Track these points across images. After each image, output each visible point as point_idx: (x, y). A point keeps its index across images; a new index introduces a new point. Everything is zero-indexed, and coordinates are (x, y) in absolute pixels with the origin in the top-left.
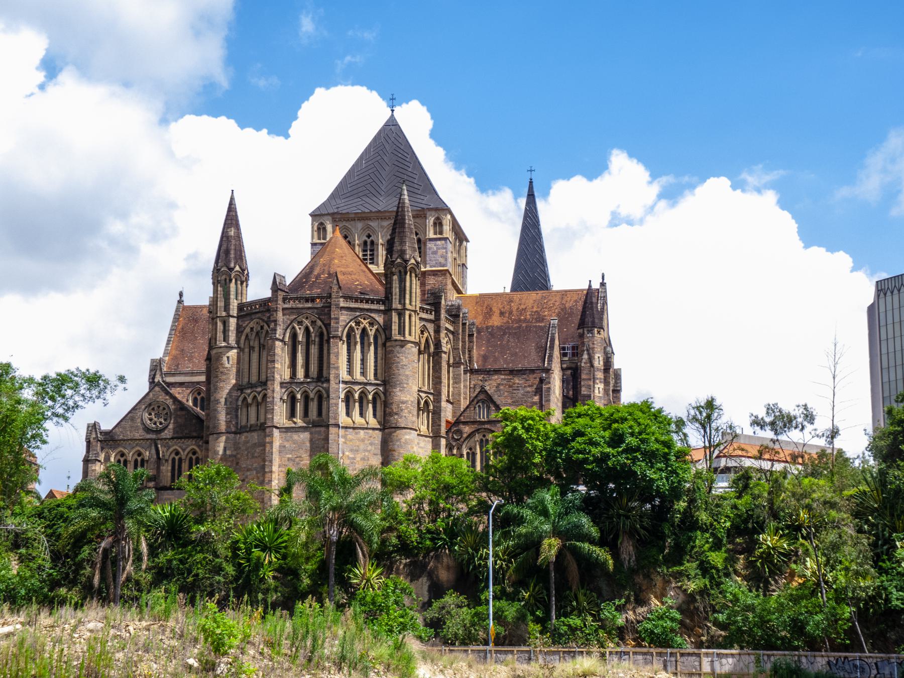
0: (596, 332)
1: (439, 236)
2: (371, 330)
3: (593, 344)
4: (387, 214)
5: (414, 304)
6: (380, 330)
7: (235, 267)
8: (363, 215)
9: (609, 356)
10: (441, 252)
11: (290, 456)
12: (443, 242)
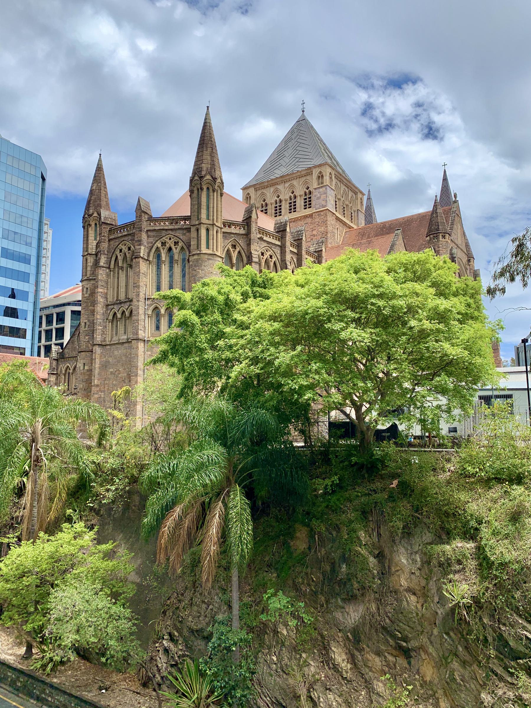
0: (441, 237)
1: (321, 185)
2: (176, 248)
3: (439, 247)
4: (288, 177)
5: (211, 218)
6: (185, 247)
7: (93, 214)
8: (273, 182)
9: (455, 256)
10: (323, 196)
11: (112, 370)
12: (324, 189)
